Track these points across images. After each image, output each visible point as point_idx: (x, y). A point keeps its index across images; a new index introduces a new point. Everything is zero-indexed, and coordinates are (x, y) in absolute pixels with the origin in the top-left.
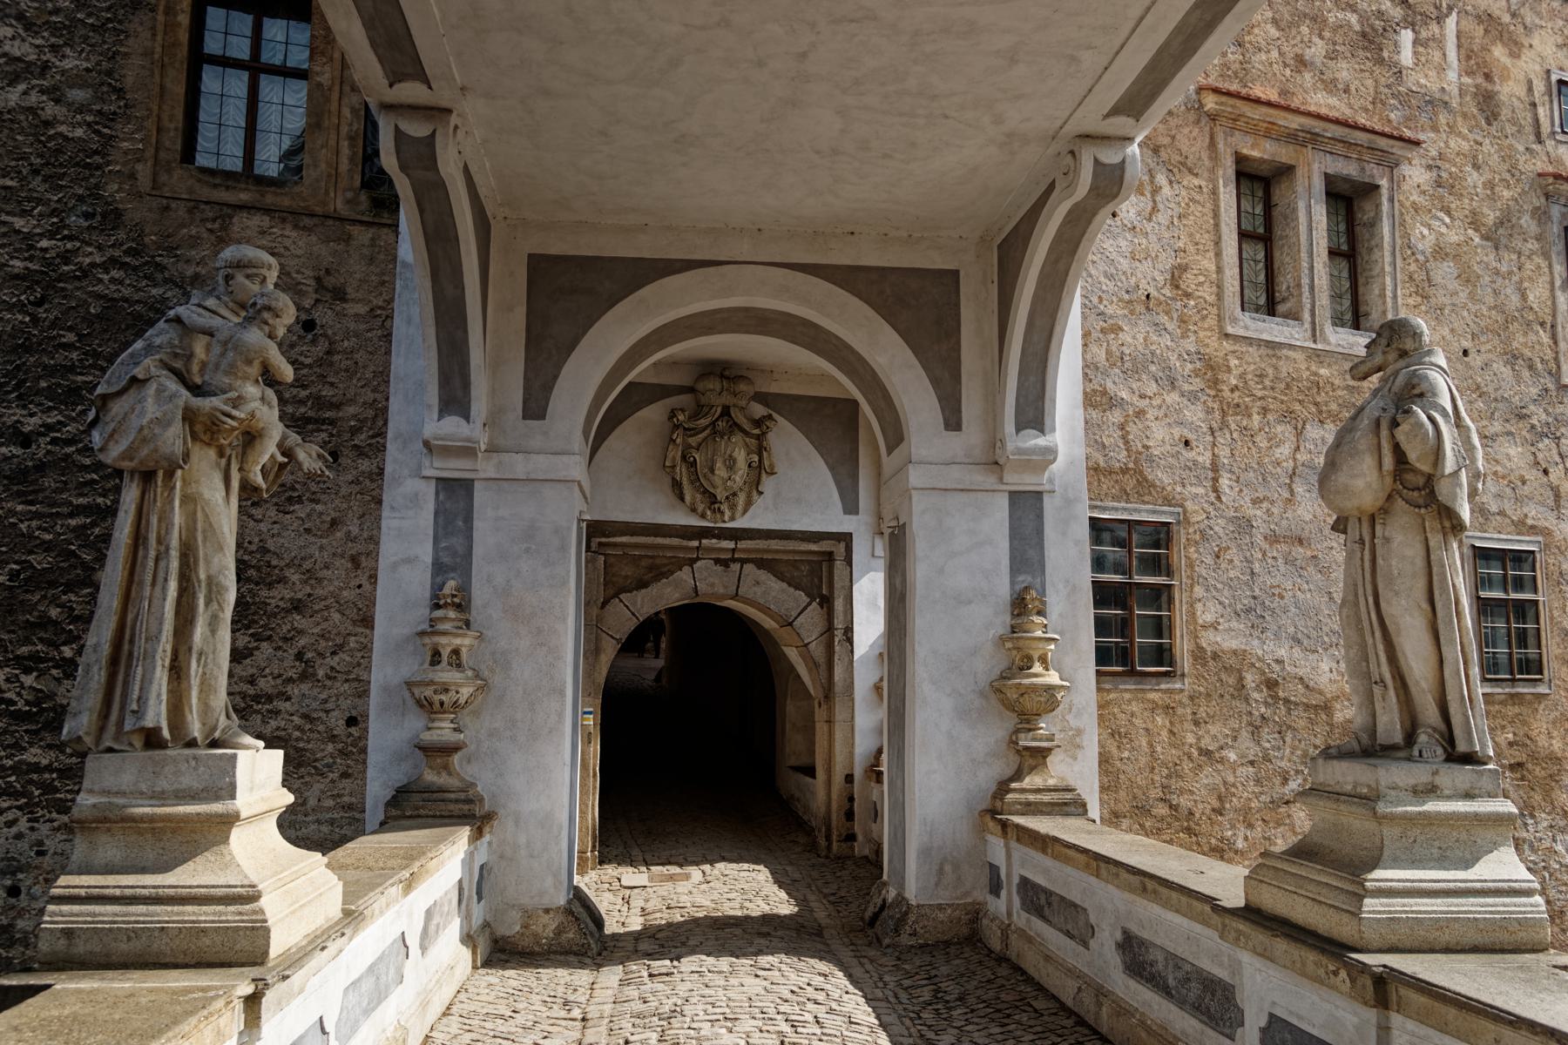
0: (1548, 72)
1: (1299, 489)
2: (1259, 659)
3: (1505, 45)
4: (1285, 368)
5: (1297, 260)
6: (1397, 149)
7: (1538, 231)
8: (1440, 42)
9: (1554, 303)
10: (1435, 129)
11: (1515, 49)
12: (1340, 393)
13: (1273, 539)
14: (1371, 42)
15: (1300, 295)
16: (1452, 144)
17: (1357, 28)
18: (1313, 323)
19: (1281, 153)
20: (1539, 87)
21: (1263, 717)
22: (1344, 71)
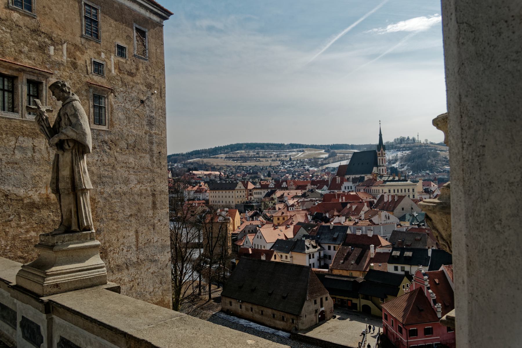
0: (91, 59)
1: (16, 152)
2: (3, 190)
3: (80, 52)
4: (13, 124)
5: (18, 99)
6: (47, 75)
7: (86, 94)
8: (62, 50)
9: (89, 111)
10: (59, 70)
11: (83, 53)
12: (29, 130)
13: (8, 163)
14: (41, 48)
15: (19, 107)
16: (64, 74)
17: (38, 45)
18: (22, 114)
19: (15, 74)
20: (88, 62)
21: (4, 203)
22: (34, 55)
